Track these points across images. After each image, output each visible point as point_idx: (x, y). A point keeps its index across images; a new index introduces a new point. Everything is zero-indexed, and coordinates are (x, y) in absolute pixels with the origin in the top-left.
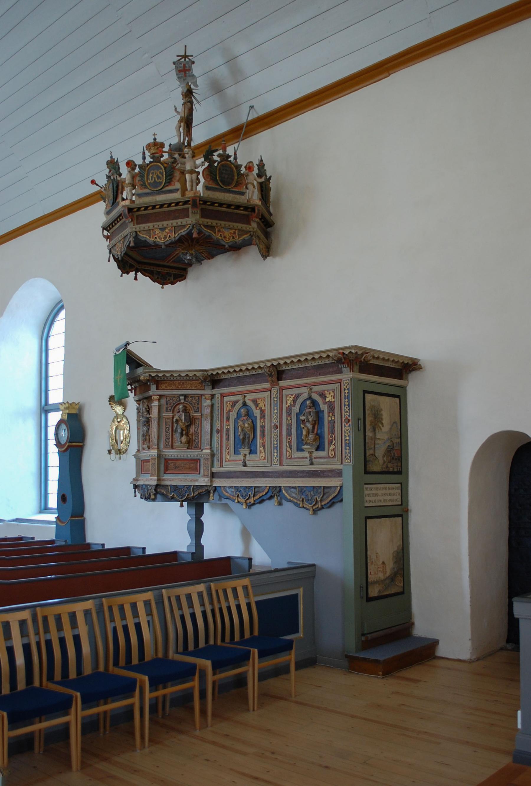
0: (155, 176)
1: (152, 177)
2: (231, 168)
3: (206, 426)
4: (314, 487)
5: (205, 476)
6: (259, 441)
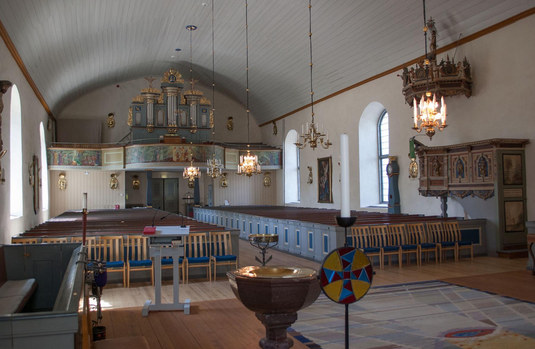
2: (451, 66)
3: (446, 167)
4: (484, 190)
5: (446, 186)
6: (465, 173)
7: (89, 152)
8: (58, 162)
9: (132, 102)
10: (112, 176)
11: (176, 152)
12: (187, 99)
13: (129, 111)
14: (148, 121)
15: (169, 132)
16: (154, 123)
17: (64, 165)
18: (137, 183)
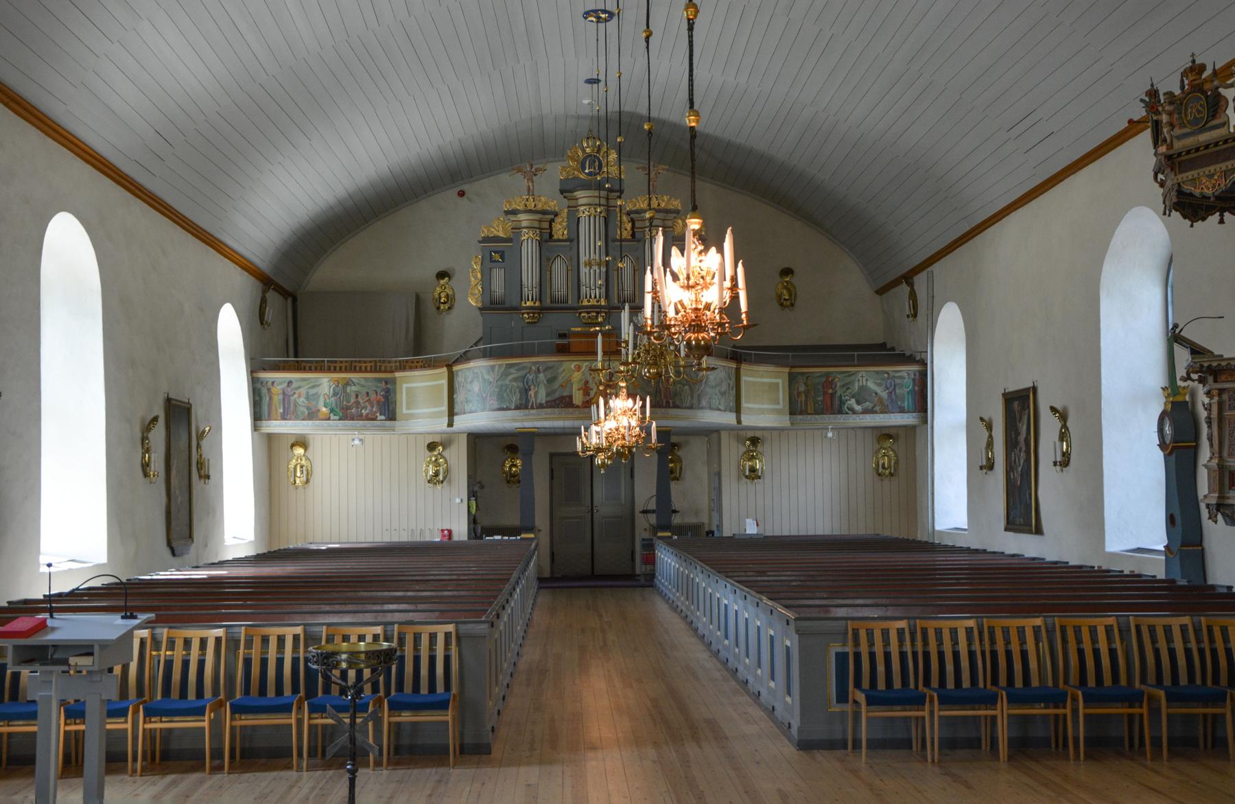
0: (1194, 111)
1: (1191, 113)
7: (363, 382)
8: (281, 410)
9: (481, 239)
10: (431, 447)
11: (581, 380)
15: (584, 321)
16: (542, 298)
17: (297, 418)
18: (515, 466)
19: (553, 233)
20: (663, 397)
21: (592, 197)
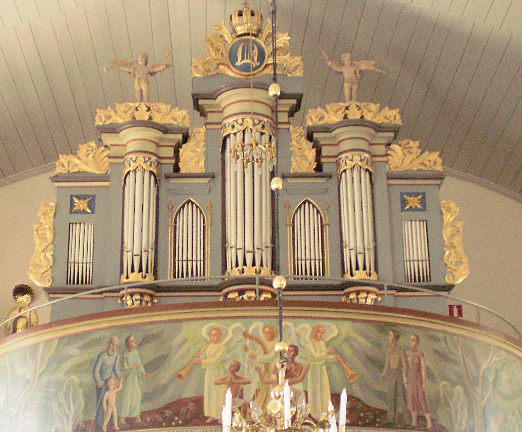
11: (223, 362)
12: (323, 148)
13: (39, 214)
14: (127, 257)
19: (180, 165)
20: (410, 406)
21: (249, 101)
